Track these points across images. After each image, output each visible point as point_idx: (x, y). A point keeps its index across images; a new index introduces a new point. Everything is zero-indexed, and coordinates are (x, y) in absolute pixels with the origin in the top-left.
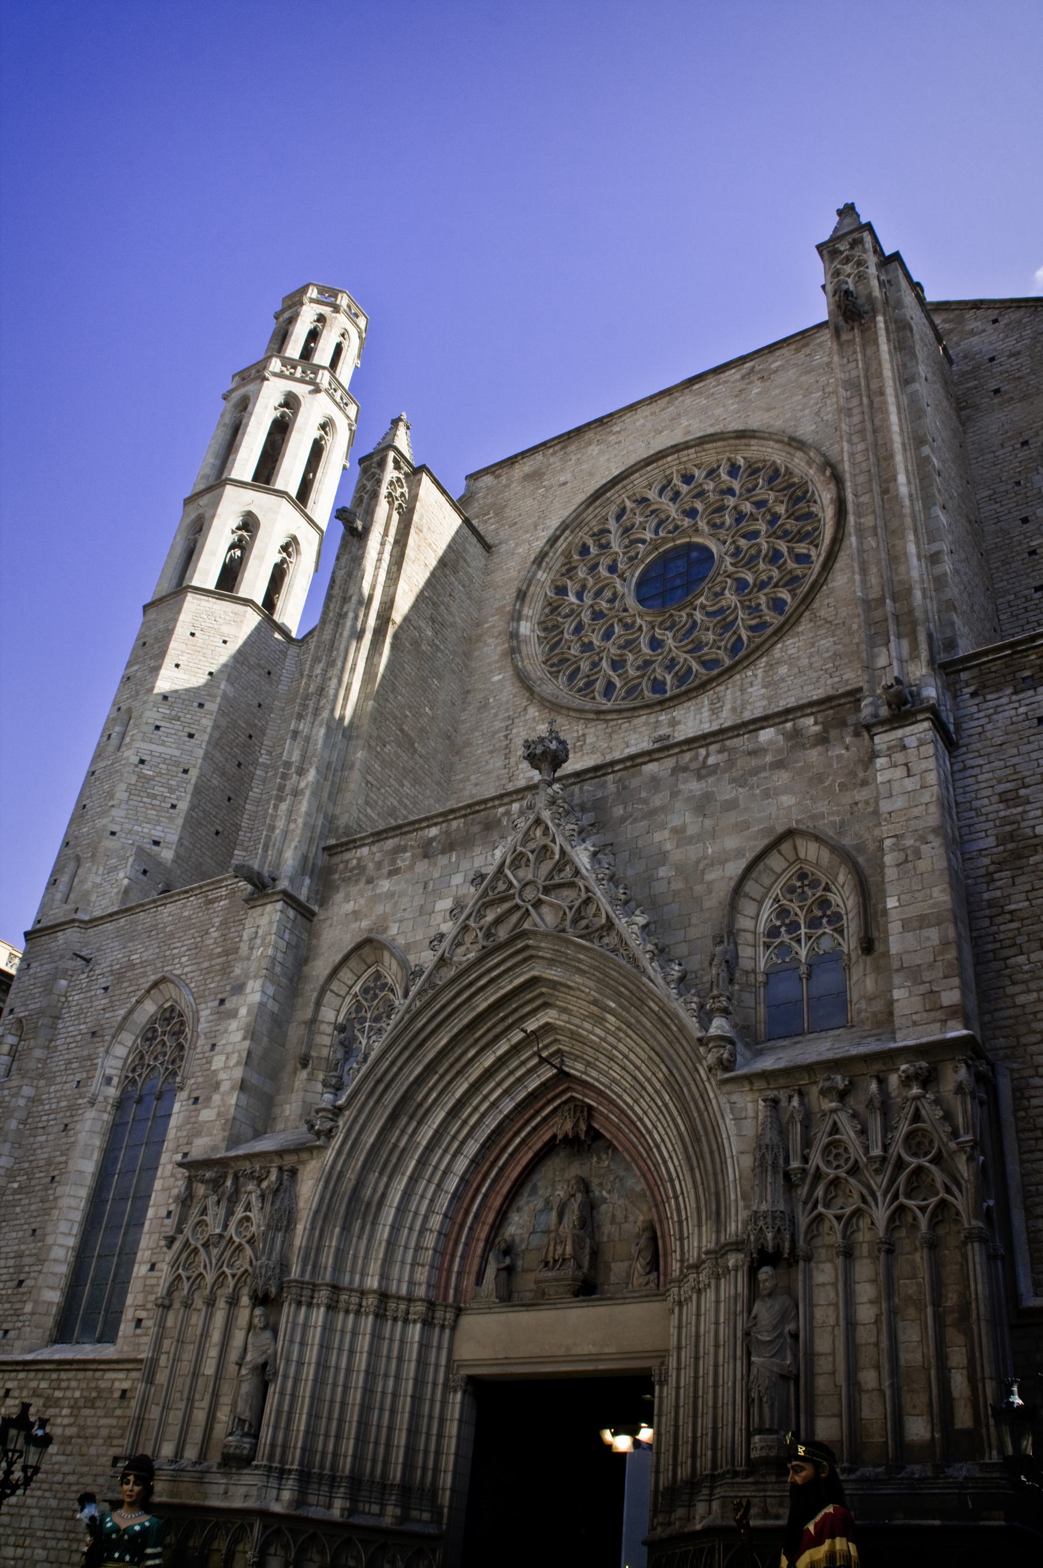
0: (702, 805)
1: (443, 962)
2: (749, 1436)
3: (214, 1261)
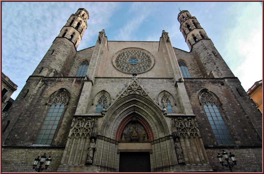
0: (152, 85)
1: (122, 95)
2: (178, 160)
3: (81, 131)
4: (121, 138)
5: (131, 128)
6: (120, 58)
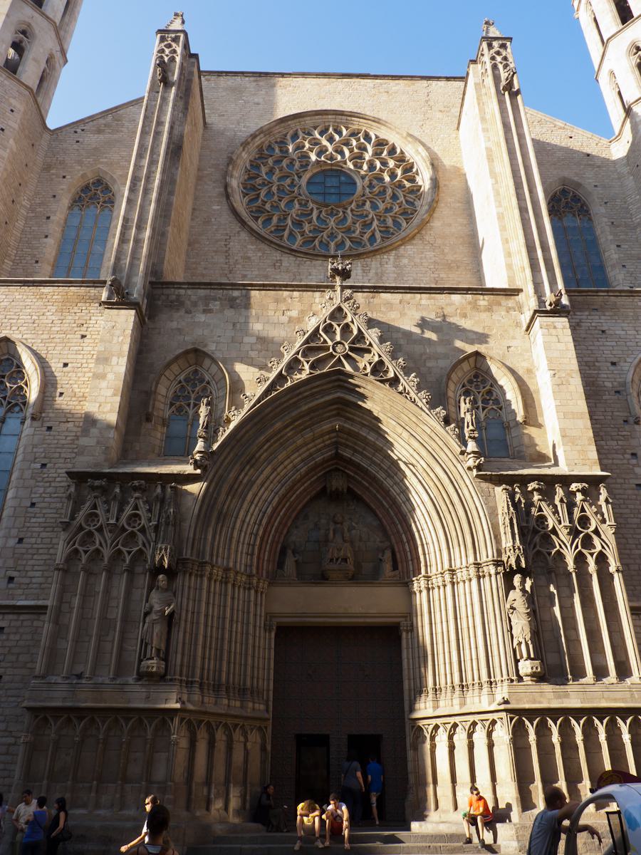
3: (109, 542)
4: (281, 565)
5: (323, 521)
6: (264, 170)
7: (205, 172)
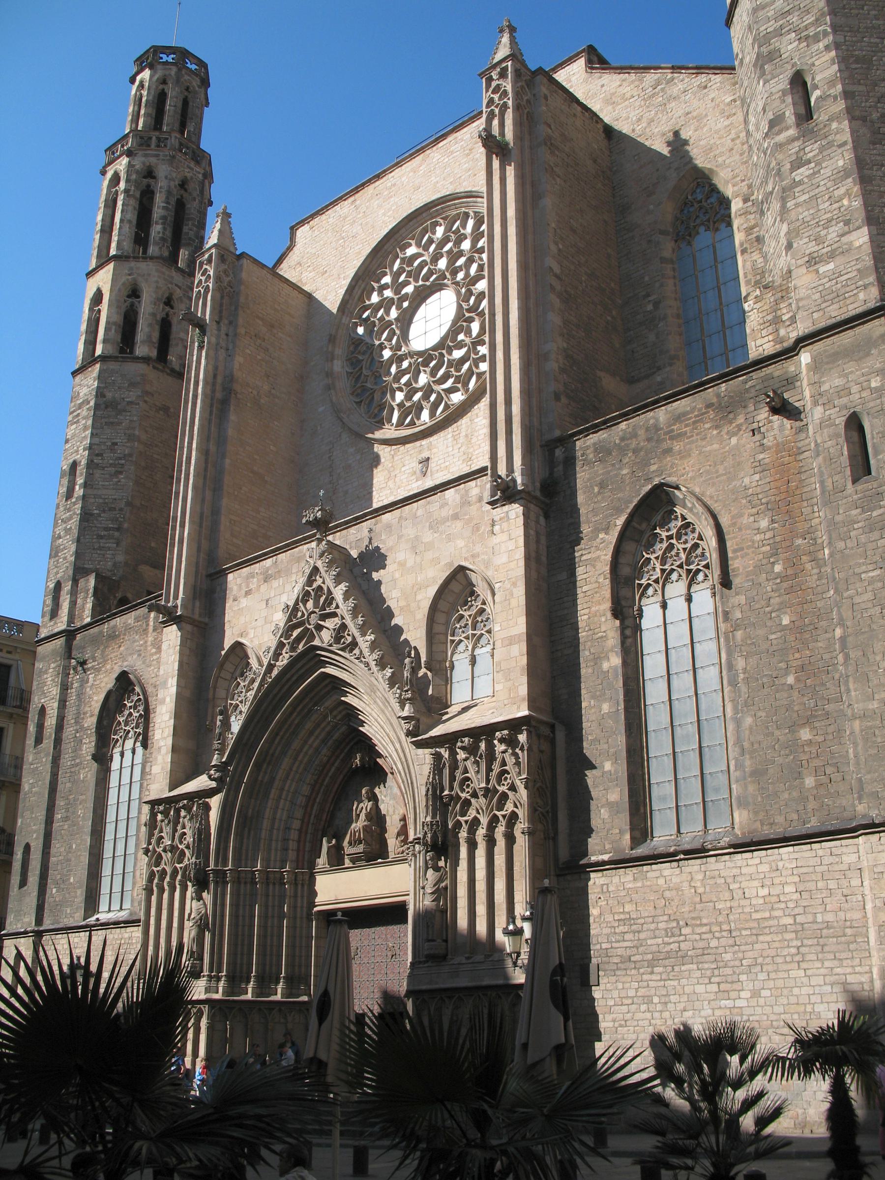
7: (312, 364)
